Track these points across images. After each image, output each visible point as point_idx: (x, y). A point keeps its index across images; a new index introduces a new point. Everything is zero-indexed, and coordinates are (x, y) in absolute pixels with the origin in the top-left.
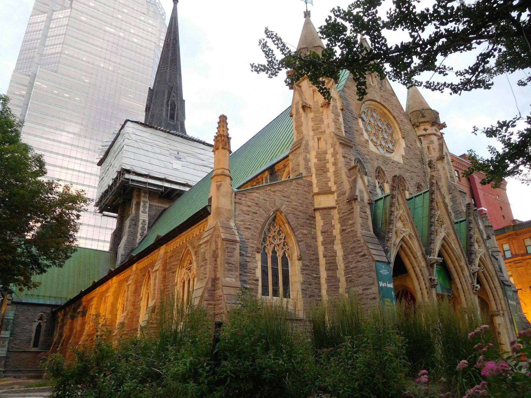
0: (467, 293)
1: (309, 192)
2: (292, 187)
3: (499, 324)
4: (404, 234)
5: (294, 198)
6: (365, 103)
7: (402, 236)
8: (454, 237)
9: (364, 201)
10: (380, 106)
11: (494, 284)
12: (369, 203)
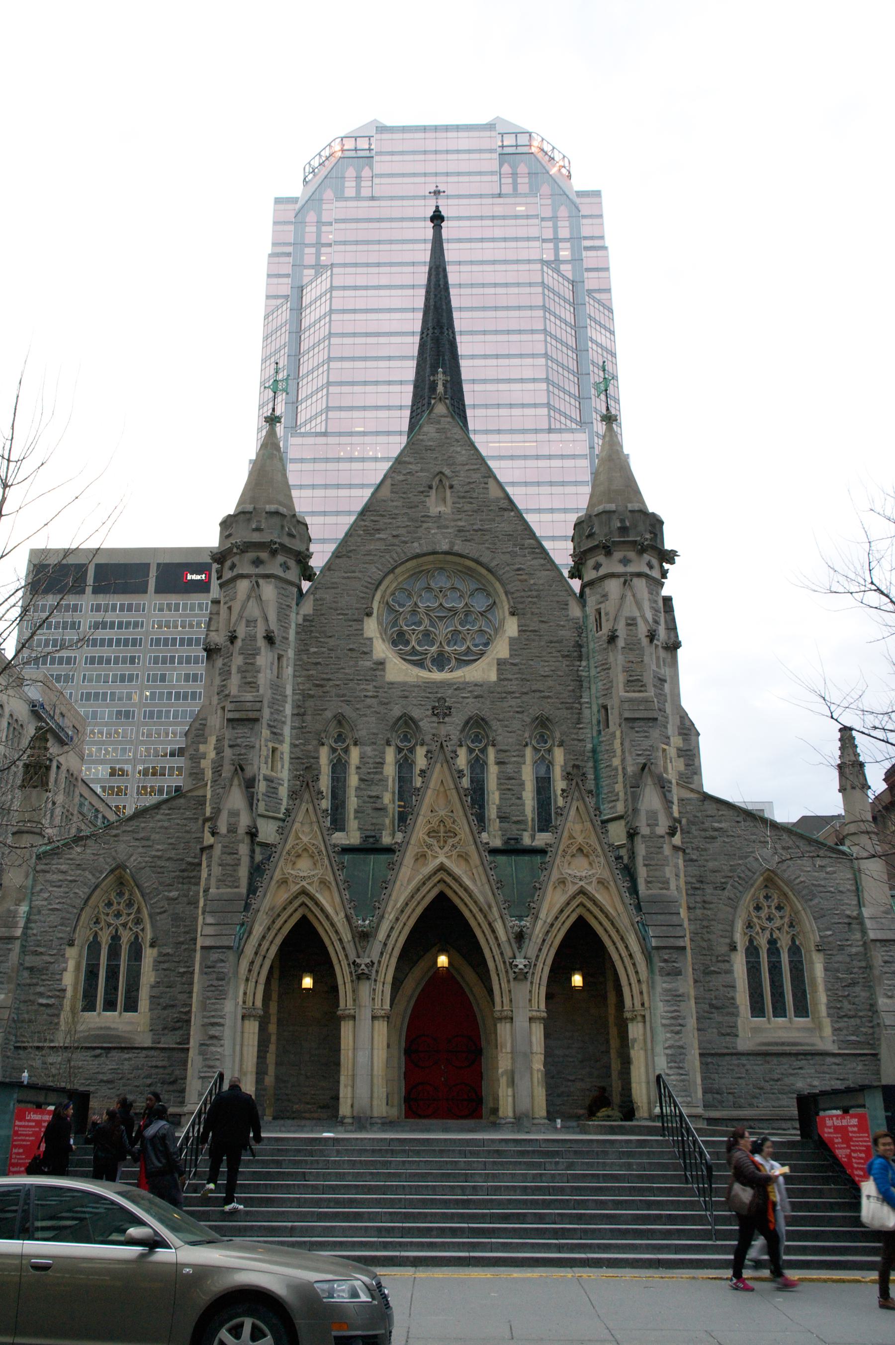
0: (503, 975)
1: (197, 819)
2: (159, 817)
3: (635, 1040)
4: (304, 883)
5: (153, 836)
6: (397, 571)
7: (295, 889)
8: (478, 862)
9: (236, 832)
10: (450, 558)
11: (627, 947)
12: (247, 833)
